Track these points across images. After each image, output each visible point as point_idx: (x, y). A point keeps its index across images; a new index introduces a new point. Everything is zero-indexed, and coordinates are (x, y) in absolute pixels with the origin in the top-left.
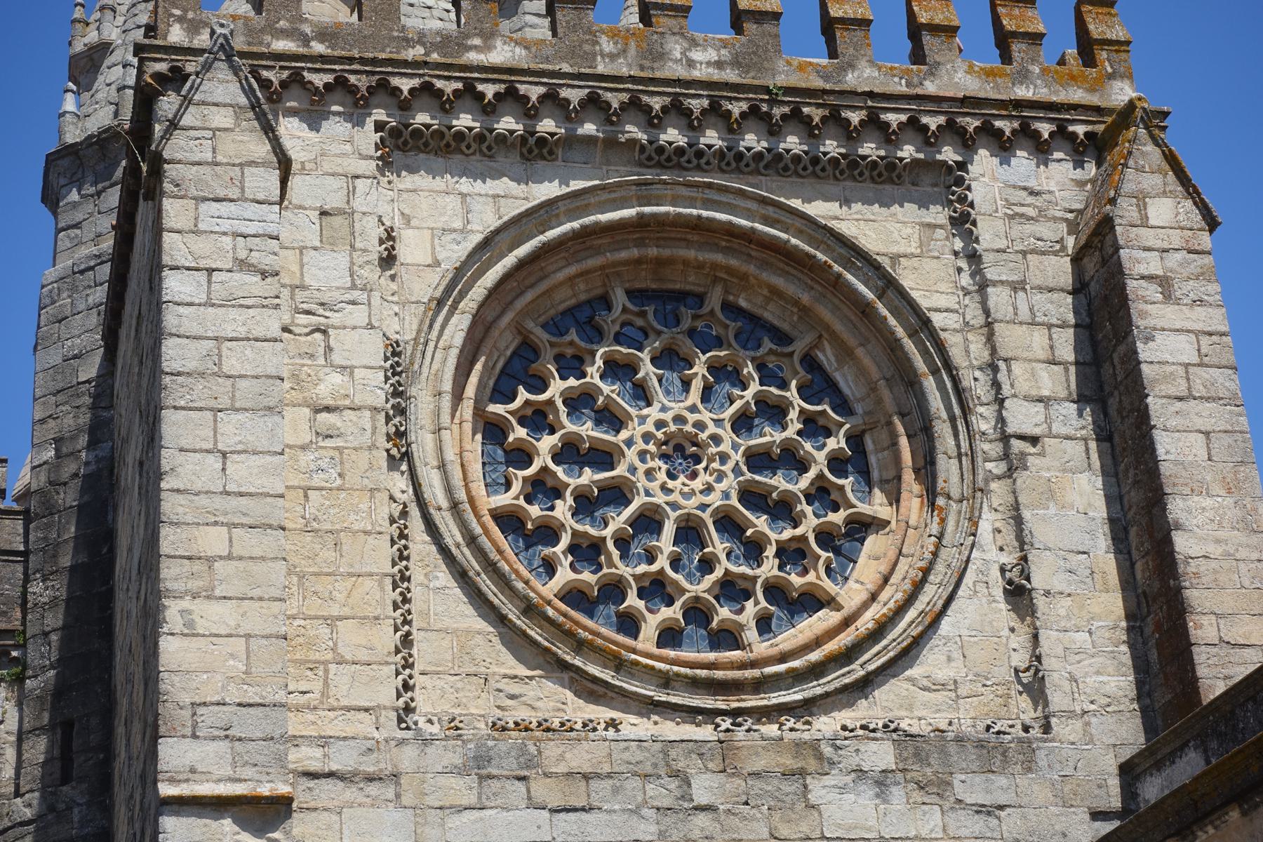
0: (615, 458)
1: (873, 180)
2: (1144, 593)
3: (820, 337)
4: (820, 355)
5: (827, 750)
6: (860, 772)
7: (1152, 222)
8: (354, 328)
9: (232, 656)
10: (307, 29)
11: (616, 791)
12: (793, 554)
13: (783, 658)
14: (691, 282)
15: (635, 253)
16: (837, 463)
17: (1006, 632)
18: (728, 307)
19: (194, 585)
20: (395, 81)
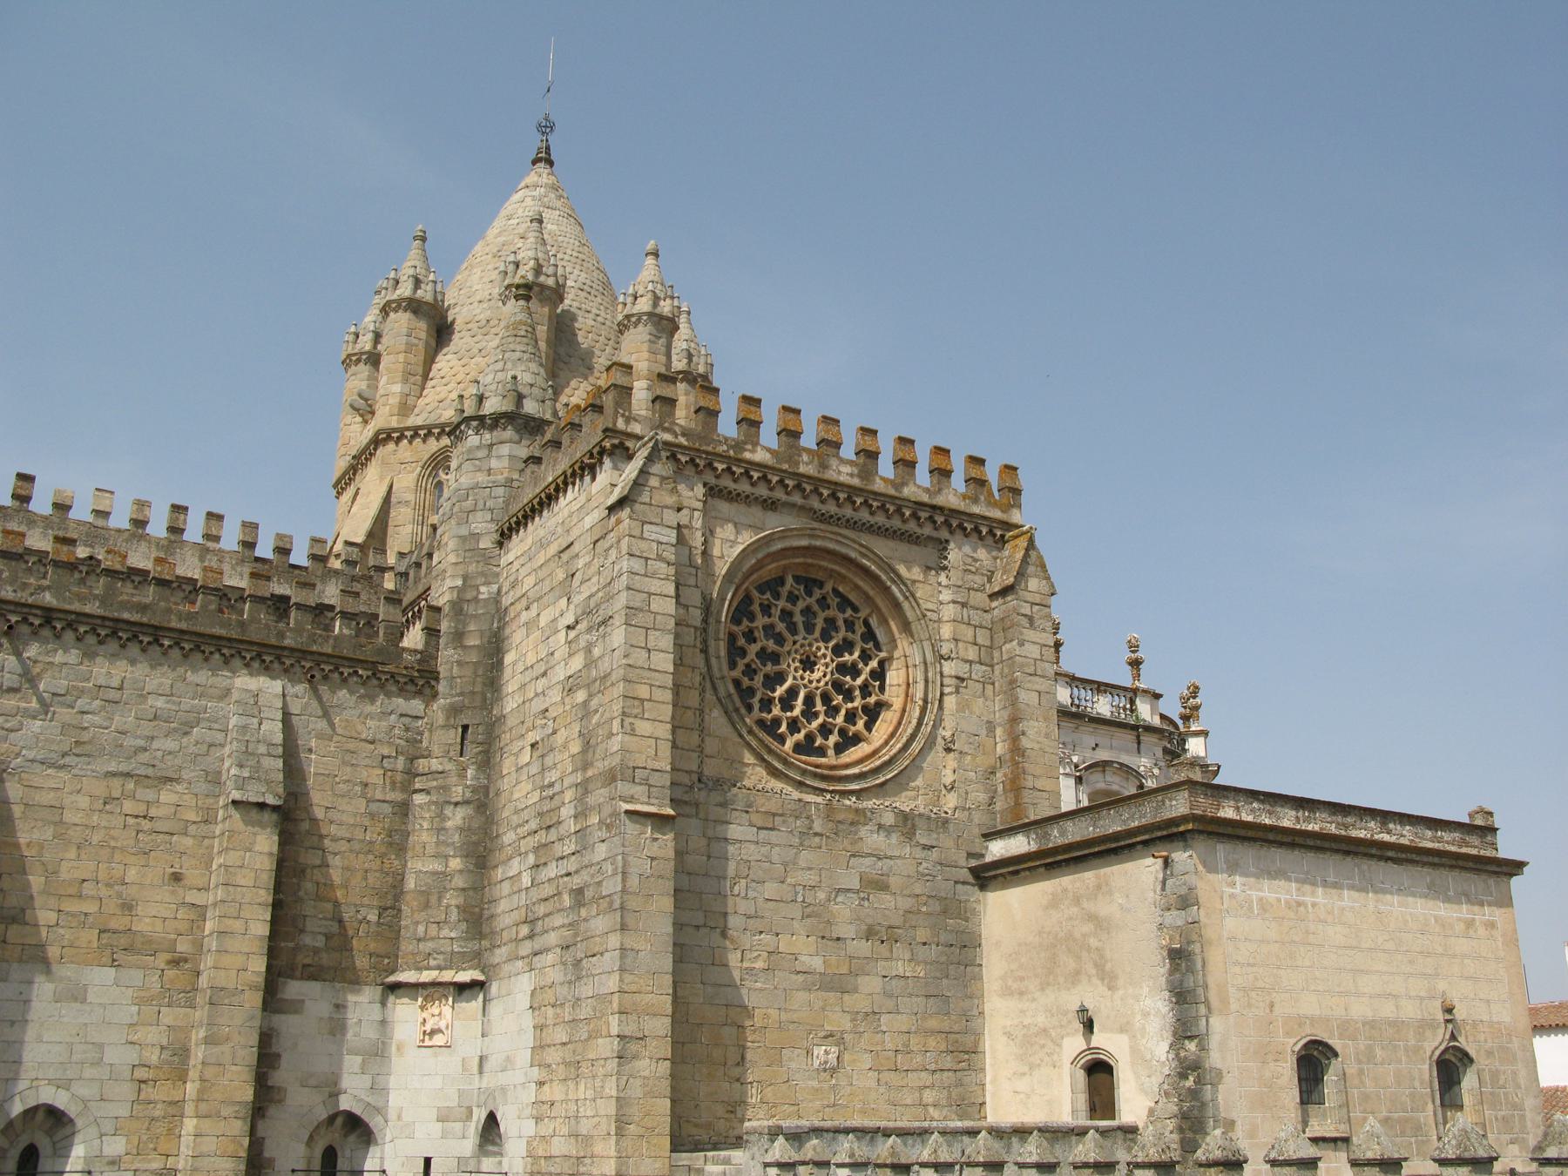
0: (781, 659)
1: (908, 541)
2: (1000, 758)
3: (873, 611)
4: (871, 620)
5: (869, 814)
6: (880, 826)
7: (1029, 589)
8: (689, 586)
9: (650, 747)
10: (677, 429)
11: (784, 822)
13: (847, 766)
14: (820, 576)
15: (801, 560)
16: (873, 673)
17: (941, 767)
18: (835, 591)
19: (635, 711)
20: (716, 465)
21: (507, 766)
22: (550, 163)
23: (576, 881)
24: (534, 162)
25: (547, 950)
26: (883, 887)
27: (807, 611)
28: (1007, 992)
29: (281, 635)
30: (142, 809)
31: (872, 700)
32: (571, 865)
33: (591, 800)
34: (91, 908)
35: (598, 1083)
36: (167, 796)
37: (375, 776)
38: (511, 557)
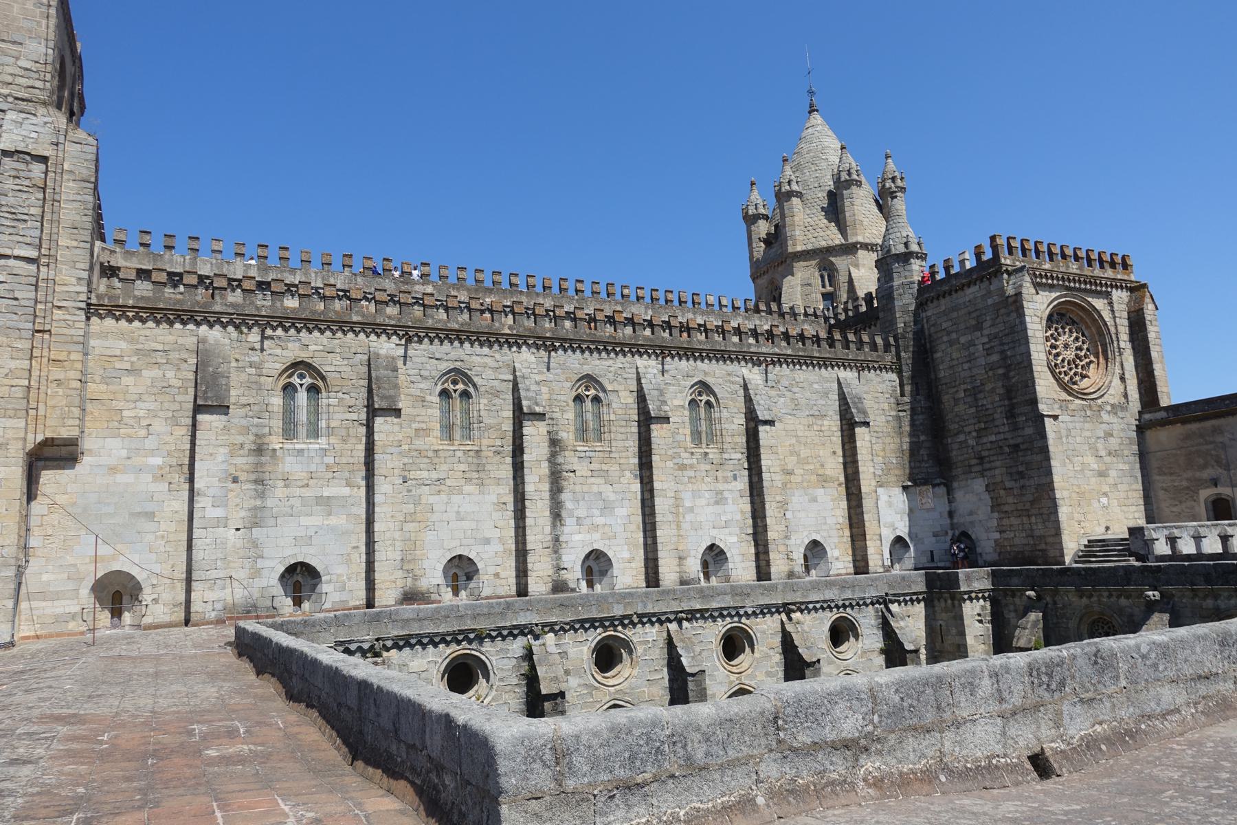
12: (1083, 367)
14: (1063, 312)
21: (945, 398)
22: (817, 111)
23: (1012, 442)
24: (810, 112)
25: (995, 468)
26: (1112, 436)
27: (1063, 328)
28: (1162, 473)
29: (848, 355)
30: (819, 428)
31: (1088, 360)
32: (1008, 436)
33: (1017, 411)
34: (812, 467)
35: (1044, 516)
36: (826, 423)
37: (886, 407)
38: (929, 313)
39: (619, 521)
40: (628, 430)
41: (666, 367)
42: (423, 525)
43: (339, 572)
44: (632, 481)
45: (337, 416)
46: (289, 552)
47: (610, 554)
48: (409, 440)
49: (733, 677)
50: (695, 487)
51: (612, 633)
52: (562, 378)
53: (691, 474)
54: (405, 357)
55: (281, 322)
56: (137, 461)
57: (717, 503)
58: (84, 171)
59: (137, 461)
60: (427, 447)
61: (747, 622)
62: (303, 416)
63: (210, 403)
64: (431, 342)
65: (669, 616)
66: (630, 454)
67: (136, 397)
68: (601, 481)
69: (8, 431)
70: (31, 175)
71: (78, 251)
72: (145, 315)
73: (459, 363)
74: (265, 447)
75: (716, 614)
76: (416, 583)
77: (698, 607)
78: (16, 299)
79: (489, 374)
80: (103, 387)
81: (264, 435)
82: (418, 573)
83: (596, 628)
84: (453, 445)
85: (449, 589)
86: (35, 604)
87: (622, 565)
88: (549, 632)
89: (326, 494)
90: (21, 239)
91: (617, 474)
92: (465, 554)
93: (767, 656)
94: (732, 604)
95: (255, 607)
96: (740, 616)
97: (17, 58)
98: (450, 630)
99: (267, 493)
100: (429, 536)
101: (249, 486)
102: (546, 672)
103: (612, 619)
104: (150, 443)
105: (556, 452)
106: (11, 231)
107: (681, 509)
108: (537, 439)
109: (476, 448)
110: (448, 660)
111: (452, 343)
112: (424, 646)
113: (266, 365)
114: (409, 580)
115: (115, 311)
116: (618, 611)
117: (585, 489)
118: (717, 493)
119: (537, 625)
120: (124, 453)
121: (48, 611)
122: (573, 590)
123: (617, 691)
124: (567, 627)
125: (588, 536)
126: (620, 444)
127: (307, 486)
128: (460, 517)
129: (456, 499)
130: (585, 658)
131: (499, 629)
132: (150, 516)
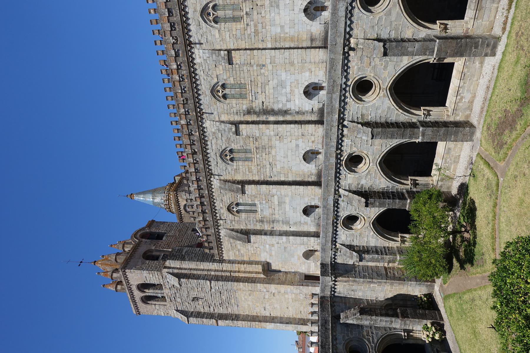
39: (289, 78)
40: (238, 69)
41: (197, 42)
42: (289, 171)
43: (307, 200)
44: (266, 68)
45: (247, 199)
46: (299, 214)
47: (306, 84)
48: (254, 175)
49: (381, 94)
50: (268, 24)
51: (344, 162)
52: (215, 107)
53: (260, 25)
54: (219, 175)
55: (214, 215)
56: (268, 250)
57: (278, 7)
58: (178, 263)
59: (268, 250)
60: (256, 169)
61: (351, 80)
62: (248, 208)
63: (247, 241)
64: (210, 166)
65: (339, 133)
66: (251, 69)
67: (247, 250)
68: (267, 87)
69: (261, 287)
70: (185, 281)
71: (204, 265)
72: (220, 249)
73: (217, 155)
74: (260, 220)
75: (343, 104)
76: (314, 174)
77: (337, 116)
78: (223, 285)
79: (219, 141)
80: (245, 257)
81: (256, 220)
82: (309, 173)
83: (340, 170)
84: (254, 157)
85: (318, 157)
86: (311, 270)
87: (313, 77)
88: (339, 192)
89: (277, 203)
90: (205, 284)
91: (263, 77)
92: (302, 155)
93: (374, 67)
94: (338, 94)
95: (317, 224)
96: (347, 85)
97: (150, 277)
98: (331, 228)
99: (277, 220)
100: (294, 169)
101: (275, 224)
102: (356, 202)
103: (337, 164)
104: (262, 247)
105: (254, 111)
106: (203, 285)
107: (282, 35)
108: (248, 129)
109: (255, 149)
110: (344, 227)
111: (209, 157)
112: (336, 235)
113: (231, 219)
114: (312, 177)
115: (221, 254)
116: (333, 160)
117: (271, 96)
118: (272, 6)
119: (334, 197)
120: (266, 253)
121: (313, 268)
122: (324, 105)
123: (373, 162)
124: (338, 184)
125: (297, 96)
126: (246, 74)
127: (274, 209)
128: (286, 156)
129: (278, 158)
130: (353, 176)
131: (334, 212)
132: (285, 248)
